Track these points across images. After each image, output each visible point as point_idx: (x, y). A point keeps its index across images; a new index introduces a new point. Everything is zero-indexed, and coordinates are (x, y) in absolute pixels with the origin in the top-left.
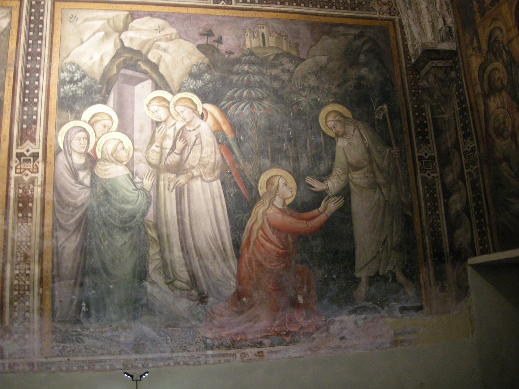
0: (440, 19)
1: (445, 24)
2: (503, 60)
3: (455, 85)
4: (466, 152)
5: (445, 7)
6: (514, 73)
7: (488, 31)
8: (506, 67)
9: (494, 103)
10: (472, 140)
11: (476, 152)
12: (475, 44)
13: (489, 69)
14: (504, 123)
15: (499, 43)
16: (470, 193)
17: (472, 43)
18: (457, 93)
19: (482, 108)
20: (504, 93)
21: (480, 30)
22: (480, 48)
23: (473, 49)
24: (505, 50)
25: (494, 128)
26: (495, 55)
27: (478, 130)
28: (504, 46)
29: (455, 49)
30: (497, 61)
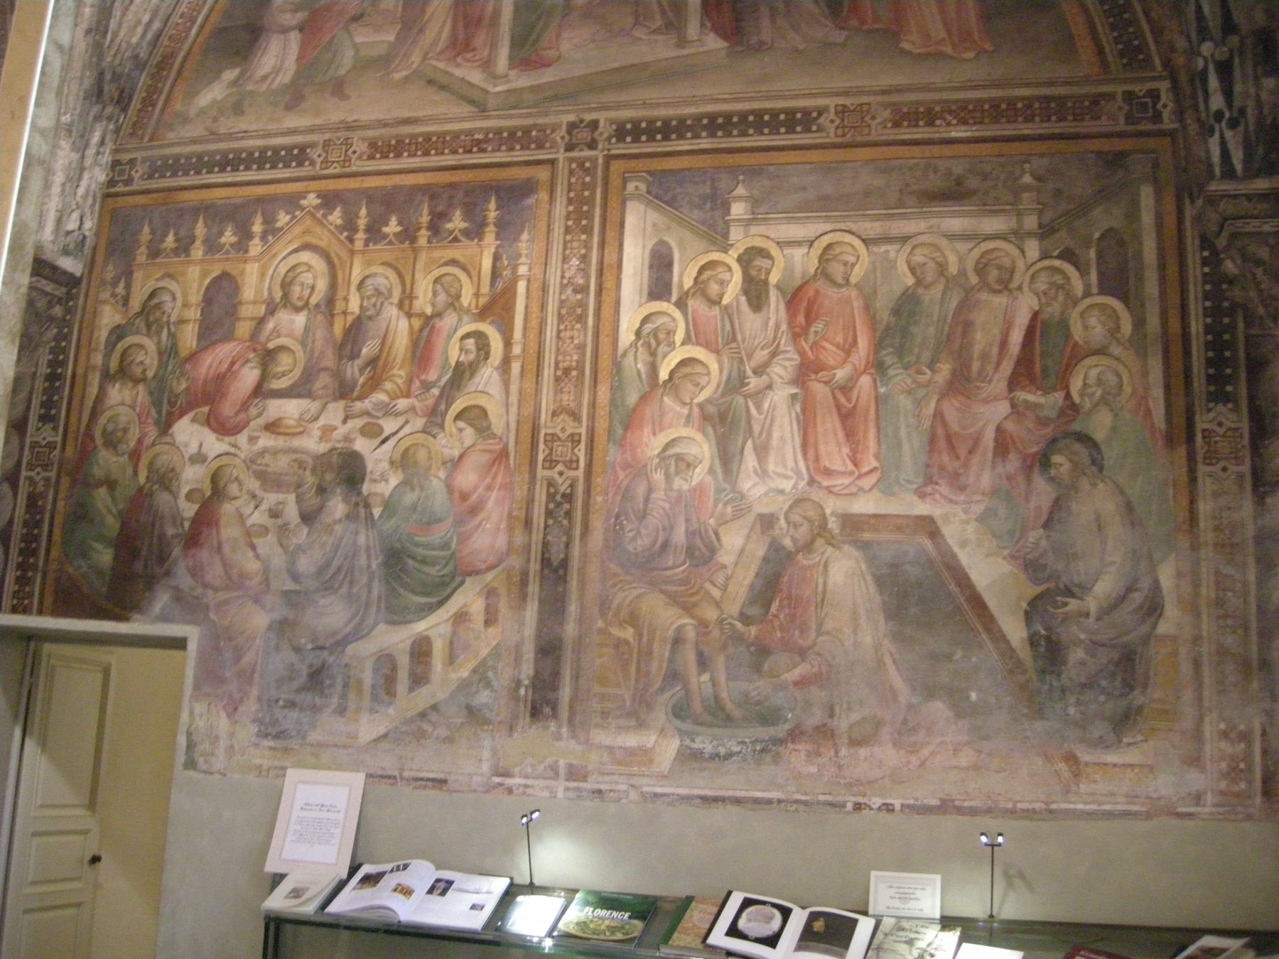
0: (75, 216)
1: (80, 228)
2: (159, 342)
3: (55, 331)
4: (34, 445)
5: (90, 201)
6: (170, 368)
7: (151, 285)
8: (160, 353)
9: (117, 394)
10: (55, 429)
11: (56, 452)
12: (120, 289)
13: (130, 340)
14: (125, 430)
15: (163, 313)
16: (20, 512)
17: (114, 285)
18: (53, 344)
19: (93, 390)
20: (141, 388)
21: (138, 275)
22: (126, 300)
23: (114, 295)
24: (169, 329)
25: (105, 430)
26: (149, 326)
27: (73, 419)
28: (168, 323)
29: (78, 274)
30: (148, 335)
